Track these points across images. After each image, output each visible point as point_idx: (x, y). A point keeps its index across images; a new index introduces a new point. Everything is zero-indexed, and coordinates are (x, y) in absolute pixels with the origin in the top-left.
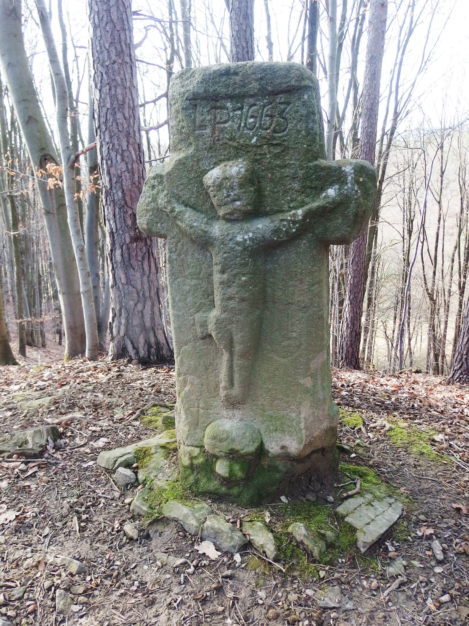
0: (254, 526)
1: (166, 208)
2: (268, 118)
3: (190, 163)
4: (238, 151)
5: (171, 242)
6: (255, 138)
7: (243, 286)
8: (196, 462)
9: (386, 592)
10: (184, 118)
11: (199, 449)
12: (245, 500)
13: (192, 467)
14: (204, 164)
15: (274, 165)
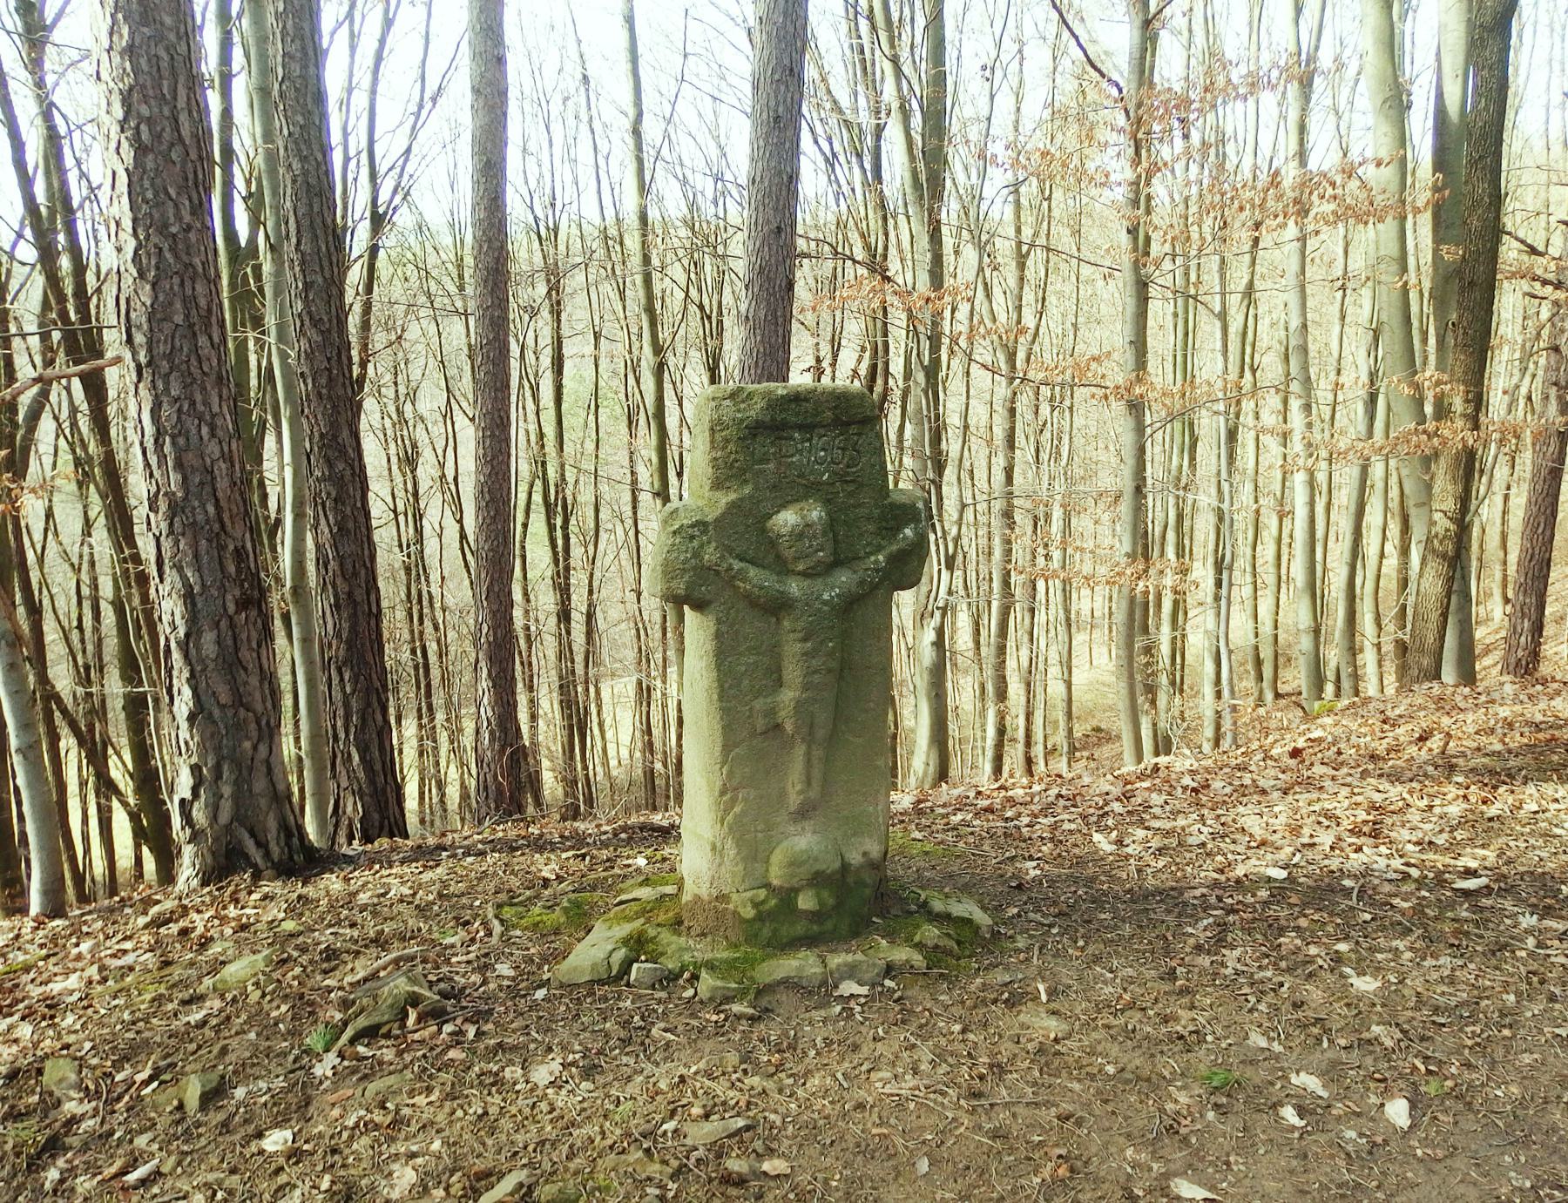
4: (807, 489)
7: (831, 654)
8: (767, 907)
13: (760, 917)
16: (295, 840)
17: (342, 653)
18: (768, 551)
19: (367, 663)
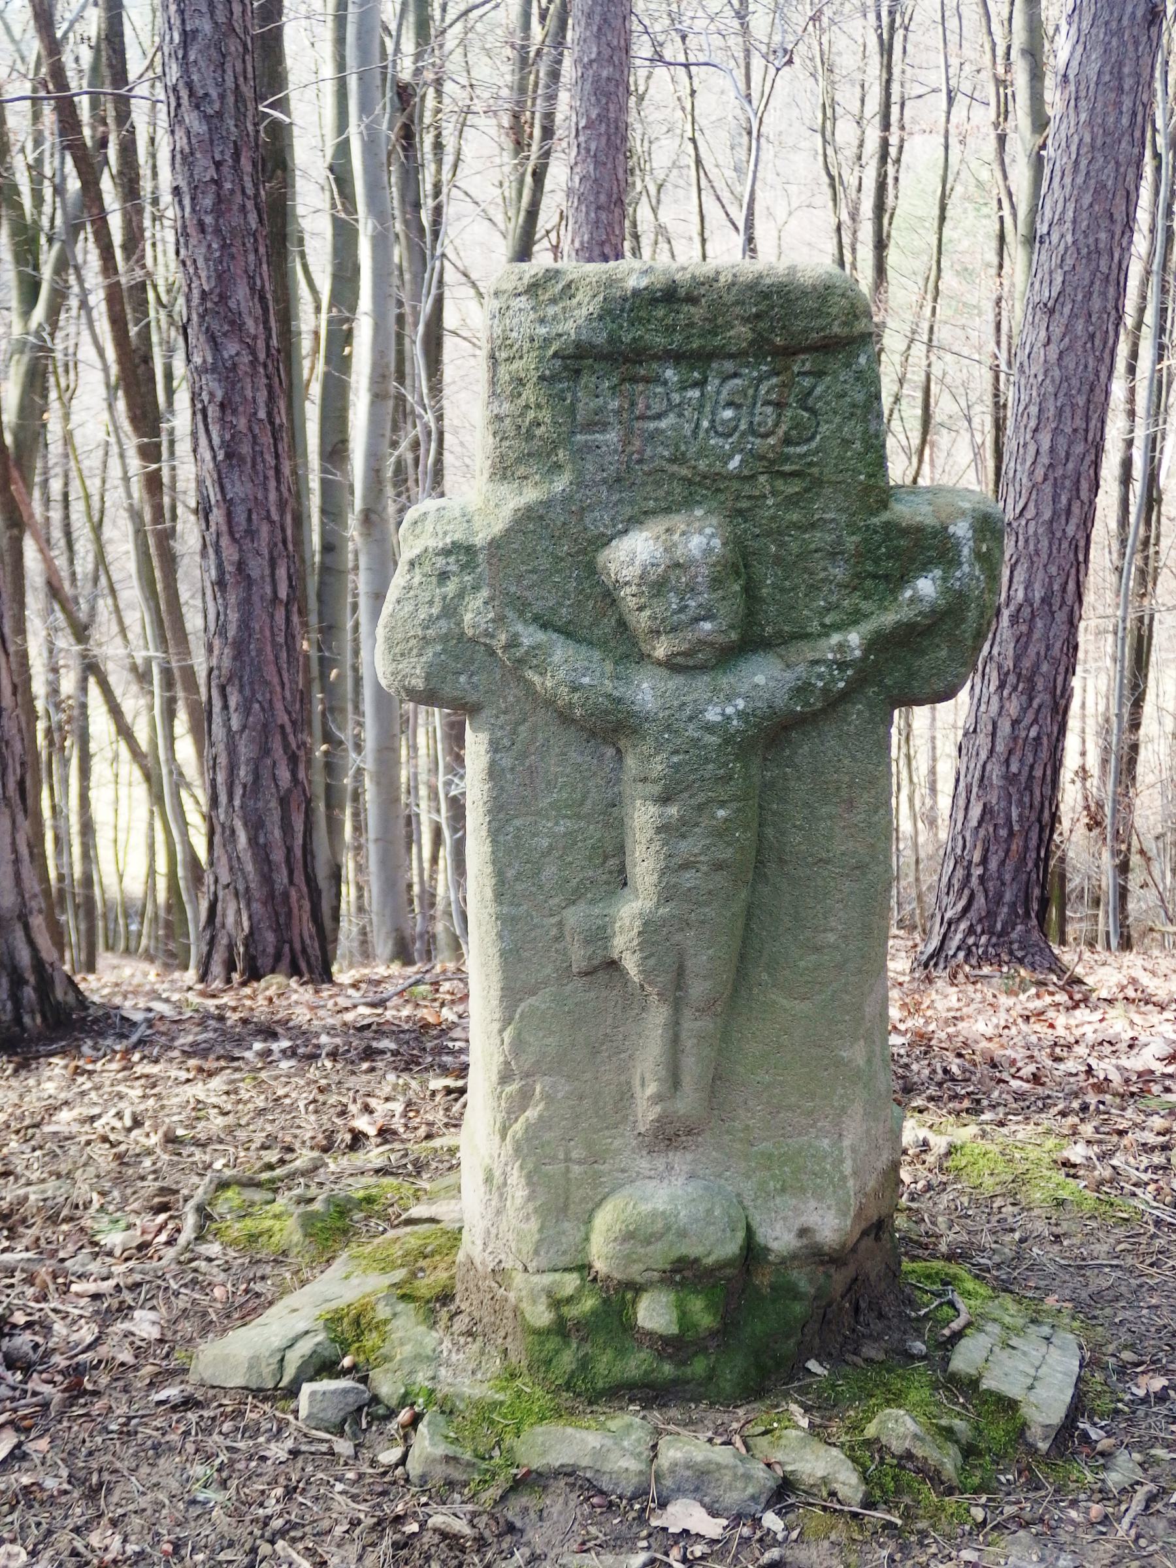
0: (783, 1442)
1: (493, 637)
2: (769, 410)
3: (557, 516)
4: (694, 488)
6: (738, 458)
7: (721, 833)
8: (573, 1312)
9: (1126, 1521)
10: (543, 402)
11: (575, 1275)
12: (728, 1387)
13: (561, 1329)
14: (596, 522)
15: (784, 524)
16: (29, 993)
17: (227, 663)
18: (596, 616)
19: (267, 683)
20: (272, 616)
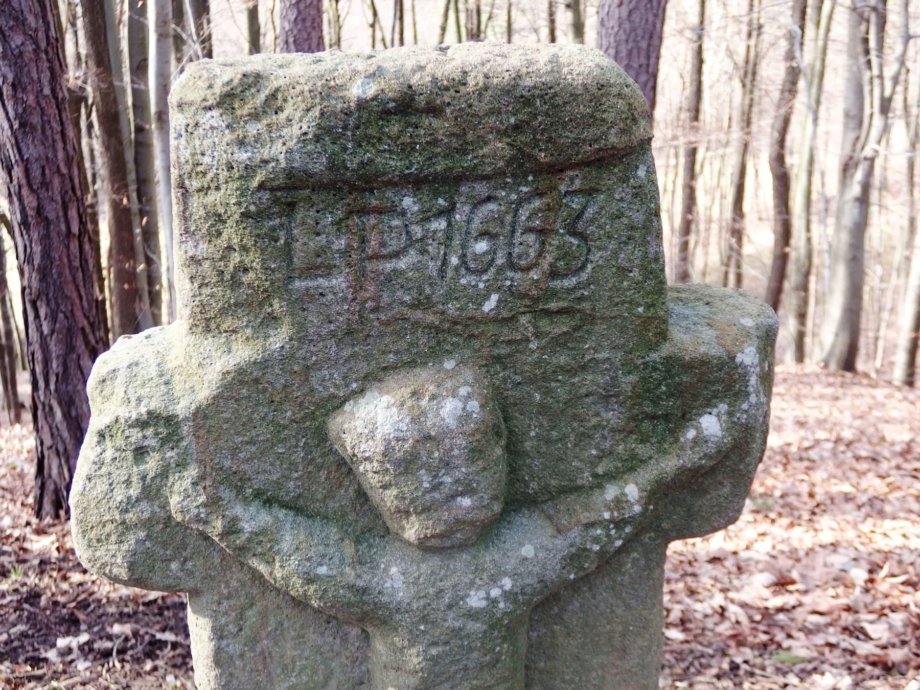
1: (206, 522)
2: (531, 238)
3: (277, 378)
5: (222, 608)
6: (494, 298)
14: (327, 381)
17: (35, 284)
18: (330, 492)
19: (68, 298)
20: (68, 247)
